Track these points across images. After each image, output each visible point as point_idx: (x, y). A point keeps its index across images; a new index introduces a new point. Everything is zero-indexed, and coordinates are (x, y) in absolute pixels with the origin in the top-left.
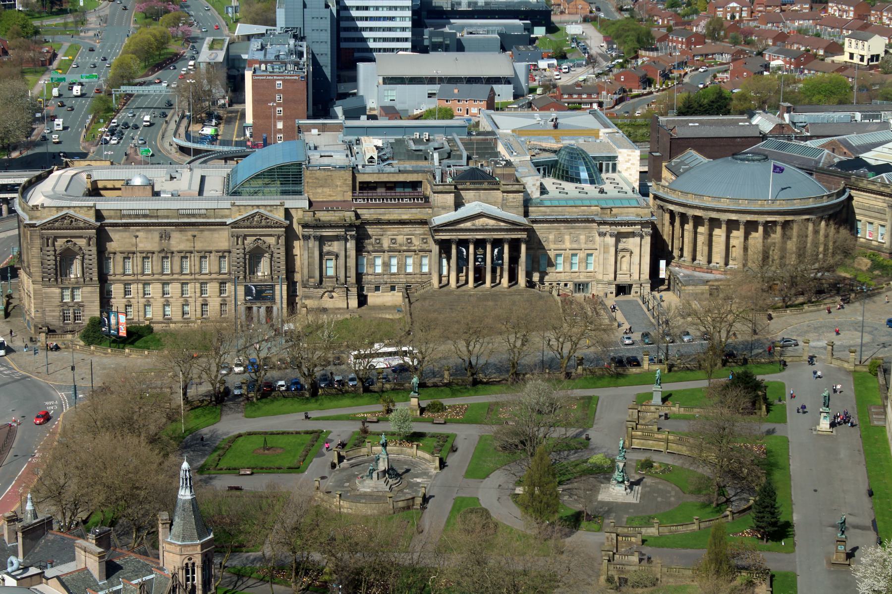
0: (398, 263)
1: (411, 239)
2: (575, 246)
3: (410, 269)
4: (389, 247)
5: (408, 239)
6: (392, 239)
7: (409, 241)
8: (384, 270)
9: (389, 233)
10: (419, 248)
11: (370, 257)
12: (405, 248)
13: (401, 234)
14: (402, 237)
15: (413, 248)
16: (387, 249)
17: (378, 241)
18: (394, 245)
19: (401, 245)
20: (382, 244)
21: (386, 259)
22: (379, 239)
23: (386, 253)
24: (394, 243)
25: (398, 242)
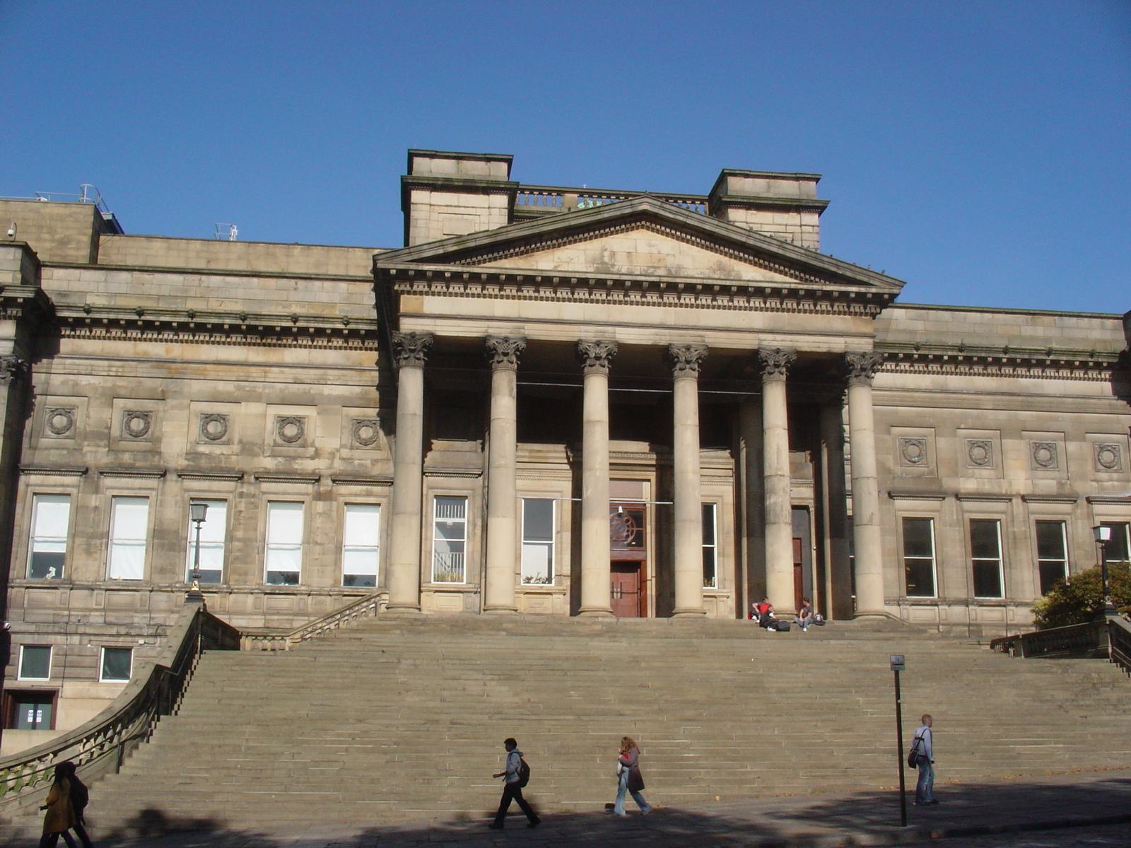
0: (230, 537)
1: (298, 421)
2: (1047, 483)
3: (282, 560)
4: (193, 455)
5: (284, 421)
6: (208, 418)
7: (291, 431)
8: (152, 569)
9: (196, 387)
10: (338, 466)
11: (94, 501)
12: (269, 463)
13: (258, 398)
14: (255, 408)
15: (309, 465)
16: (182, 463)
17: (137, 424)
18: (217, 450)
19: (248, 448)
20: (158, 440)
21: (171, 513)
22: (145, 416)
23: (173, 484)
24: (214, 439)
25: (236, 433)
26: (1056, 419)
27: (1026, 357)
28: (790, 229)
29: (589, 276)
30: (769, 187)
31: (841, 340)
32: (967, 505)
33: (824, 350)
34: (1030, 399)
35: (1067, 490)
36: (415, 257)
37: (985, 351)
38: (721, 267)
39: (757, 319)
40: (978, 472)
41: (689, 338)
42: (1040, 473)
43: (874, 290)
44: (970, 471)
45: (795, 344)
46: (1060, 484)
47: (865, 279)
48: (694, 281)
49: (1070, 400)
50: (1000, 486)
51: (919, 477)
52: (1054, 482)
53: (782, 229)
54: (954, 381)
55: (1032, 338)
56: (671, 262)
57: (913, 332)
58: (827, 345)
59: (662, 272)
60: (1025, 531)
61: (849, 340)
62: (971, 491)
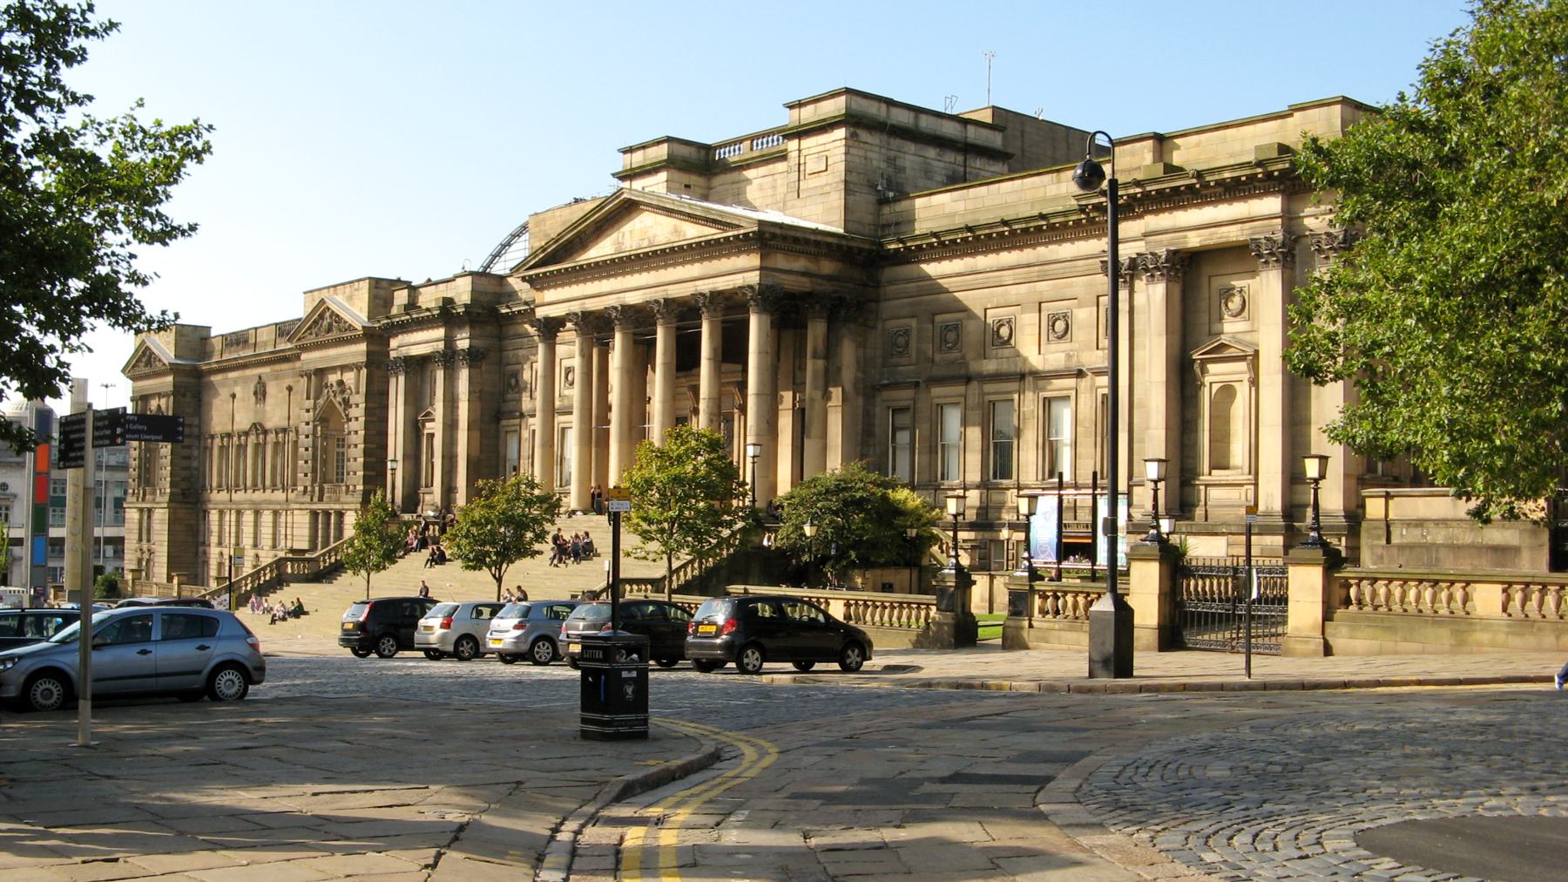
26: (1071, 285)
27: (1024, 226)
28: (828, 147)
29: (614, 256)
30: (816, 111)
31: (740, 276)
32: (988, 387)
33: (731, 287)
34: (1046, 267)
35: (1074, 364)
36: (527, 266)
37: (988, 228)
38: (676, 231)
39: (695, 269)
40: (1000, 351)
41: (658, 294)
42: (1053, 347)
43: (742, 231)
44: (994, 352)
45: (717, 285)
46: (1069, 356)
47: (737, 223)
48: (663, 247)
49: (1083, 262)
50: (1016, 365)
51: (953, 363)
52: (1063, 355)
53: (822, 148)
54: (982, 261)
55: (1055, 198)
56: (650, 234)
57: (952, 215)
58: (731, 283)
59: (646, 243)
60: (1033, 411)
61: (745, 275)
62: (991, 372)
